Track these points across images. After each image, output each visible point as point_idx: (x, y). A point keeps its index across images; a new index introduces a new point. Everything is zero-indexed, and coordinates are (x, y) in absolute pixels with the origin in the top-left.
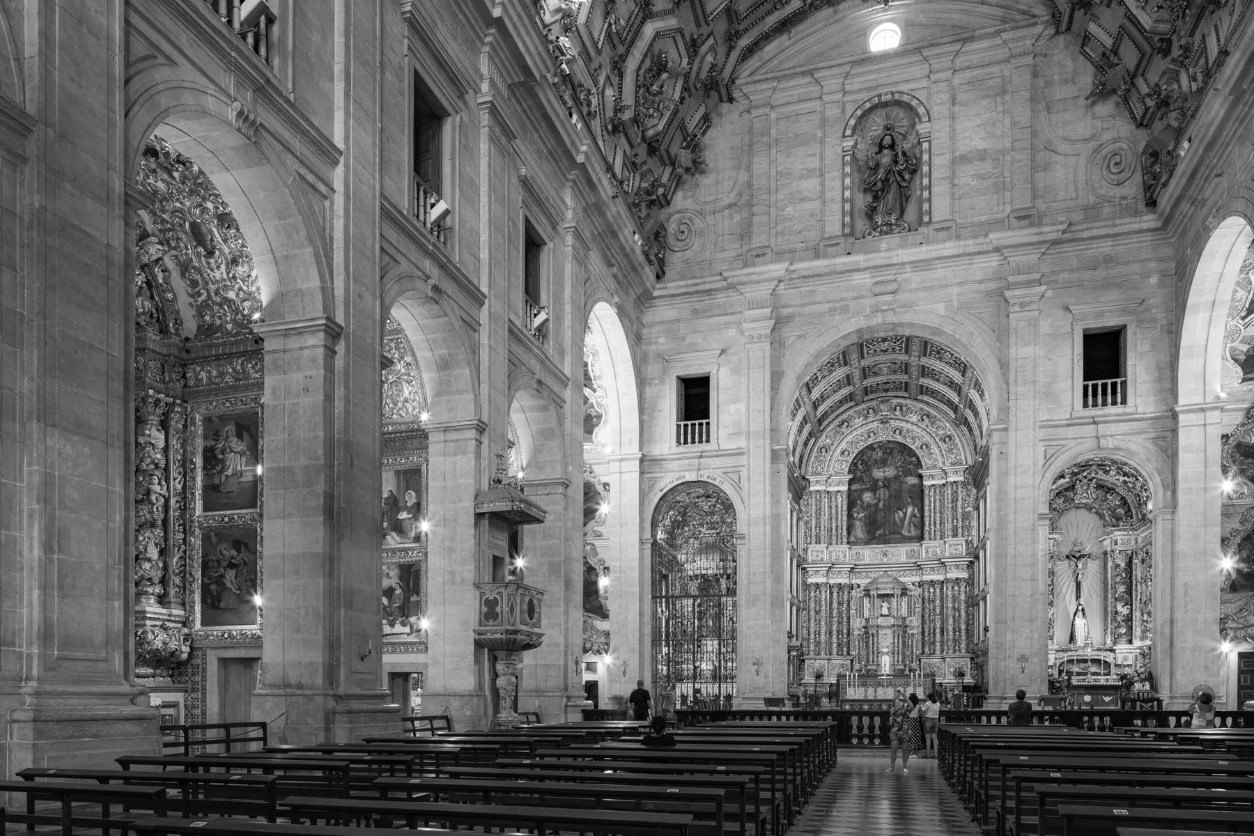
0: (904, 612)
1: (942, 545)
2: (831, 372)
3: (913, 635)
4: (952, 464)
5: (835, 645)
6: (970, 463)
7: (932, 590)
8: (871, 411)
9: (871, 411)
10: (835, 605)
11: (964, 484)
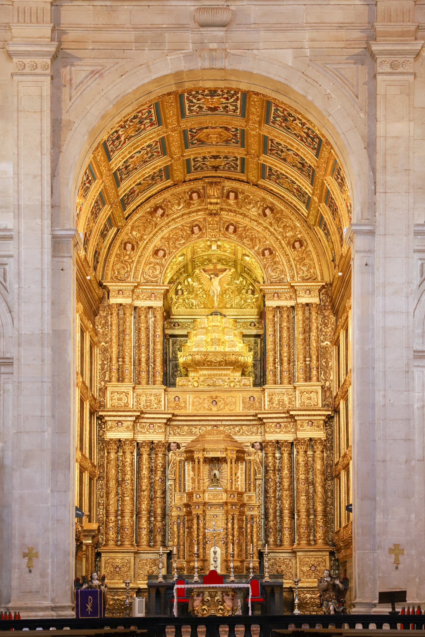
0: (241, 485)
1: (291, 391)
2: (138, 131)
3: (252, 517)
4: (304, 280)
5: (144, 532)
6: (327, 279)
7: (277, 455)
8: (195, 195)
9: (195, 195)
10: (145, 472)
11: (320, 308)
